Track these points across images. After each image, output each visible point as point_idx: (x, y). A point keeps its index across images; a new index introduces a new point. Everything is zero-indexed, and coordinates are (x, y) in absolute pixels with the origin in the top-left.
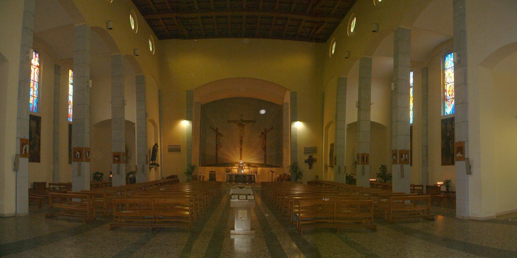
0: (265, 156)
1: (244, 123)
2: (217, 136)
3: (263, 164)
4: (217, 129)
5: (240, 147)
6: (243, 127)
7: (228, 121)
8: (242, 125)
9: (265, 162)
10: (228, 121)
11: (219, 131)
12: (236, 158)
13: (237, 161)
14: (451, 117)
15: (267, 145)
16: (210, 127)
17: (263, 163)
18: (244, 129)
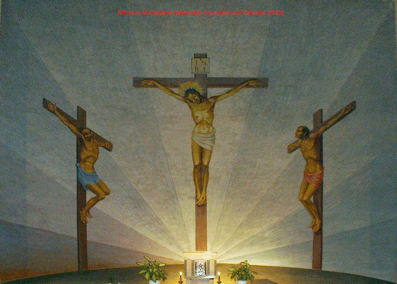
0: (319, 233)
1: (212, 92)
2: (80, 145)
3: (310, 270)
4: (82, 113)
5: (197, 200)
6: (211, 110)
7: (138, 82)
8: (203, 98)
9: (318, 260)
10: (138, 82)
11: (90, 125)
12: (179, 247)
13: (179, 257)
14: (217, 274)
15: (326, 190)
16: (46, 104)
17: (308, 265)
18: (212, 117)
